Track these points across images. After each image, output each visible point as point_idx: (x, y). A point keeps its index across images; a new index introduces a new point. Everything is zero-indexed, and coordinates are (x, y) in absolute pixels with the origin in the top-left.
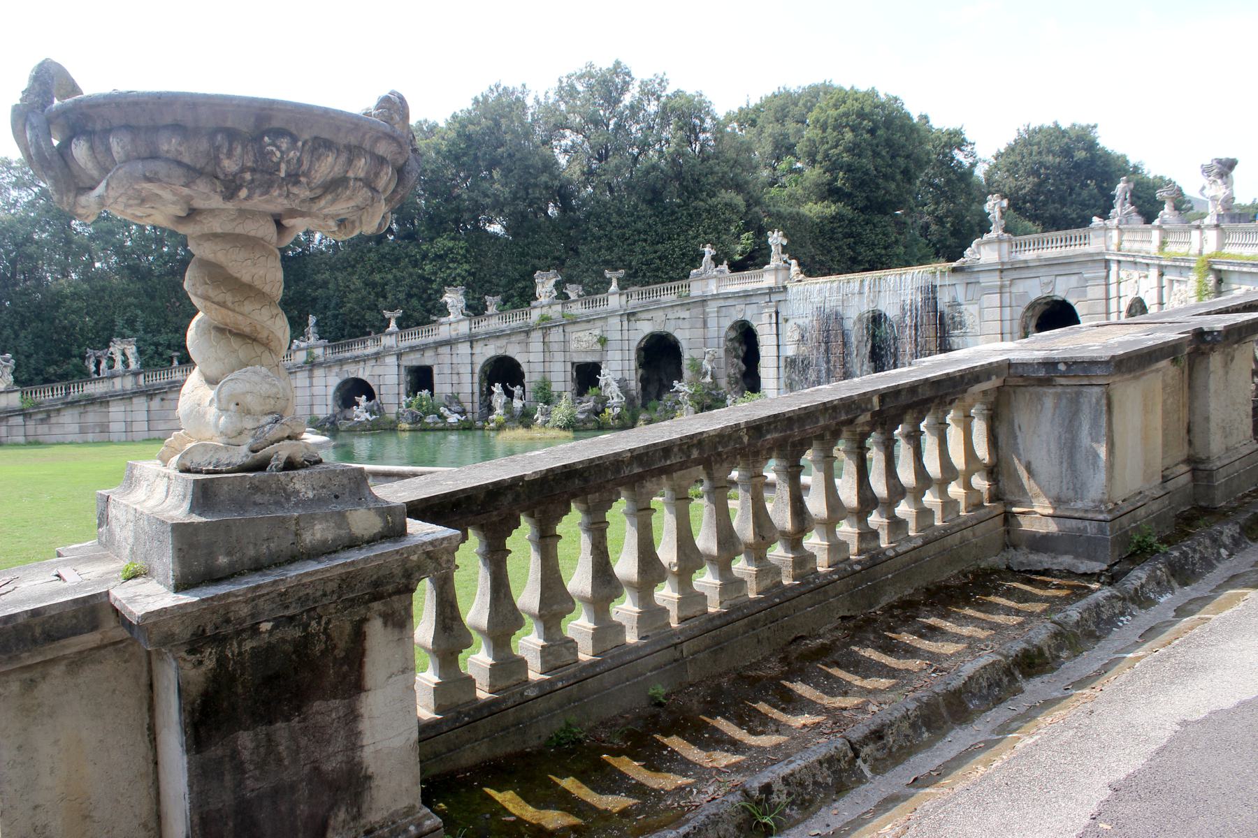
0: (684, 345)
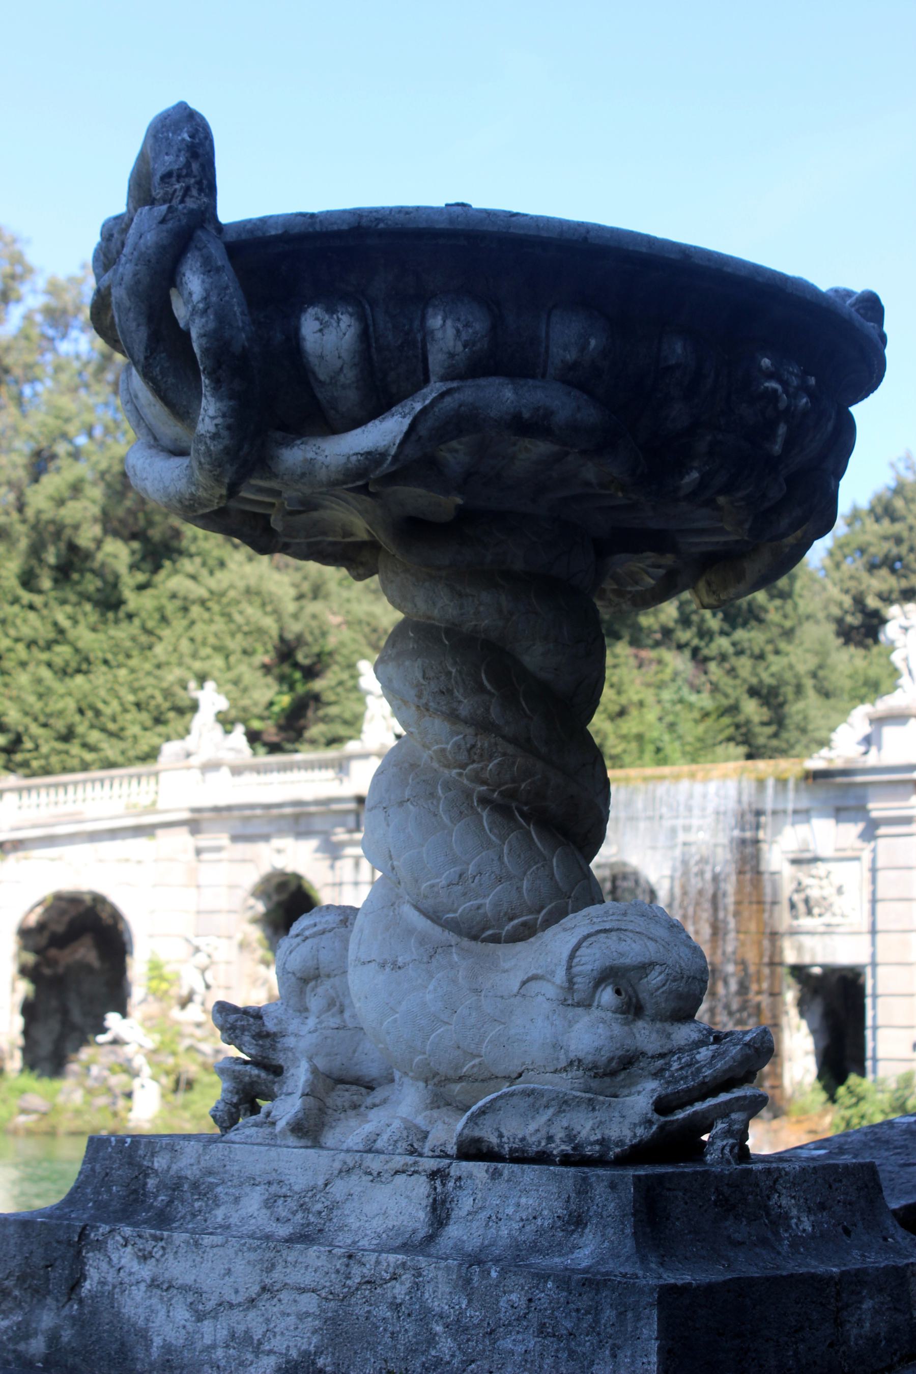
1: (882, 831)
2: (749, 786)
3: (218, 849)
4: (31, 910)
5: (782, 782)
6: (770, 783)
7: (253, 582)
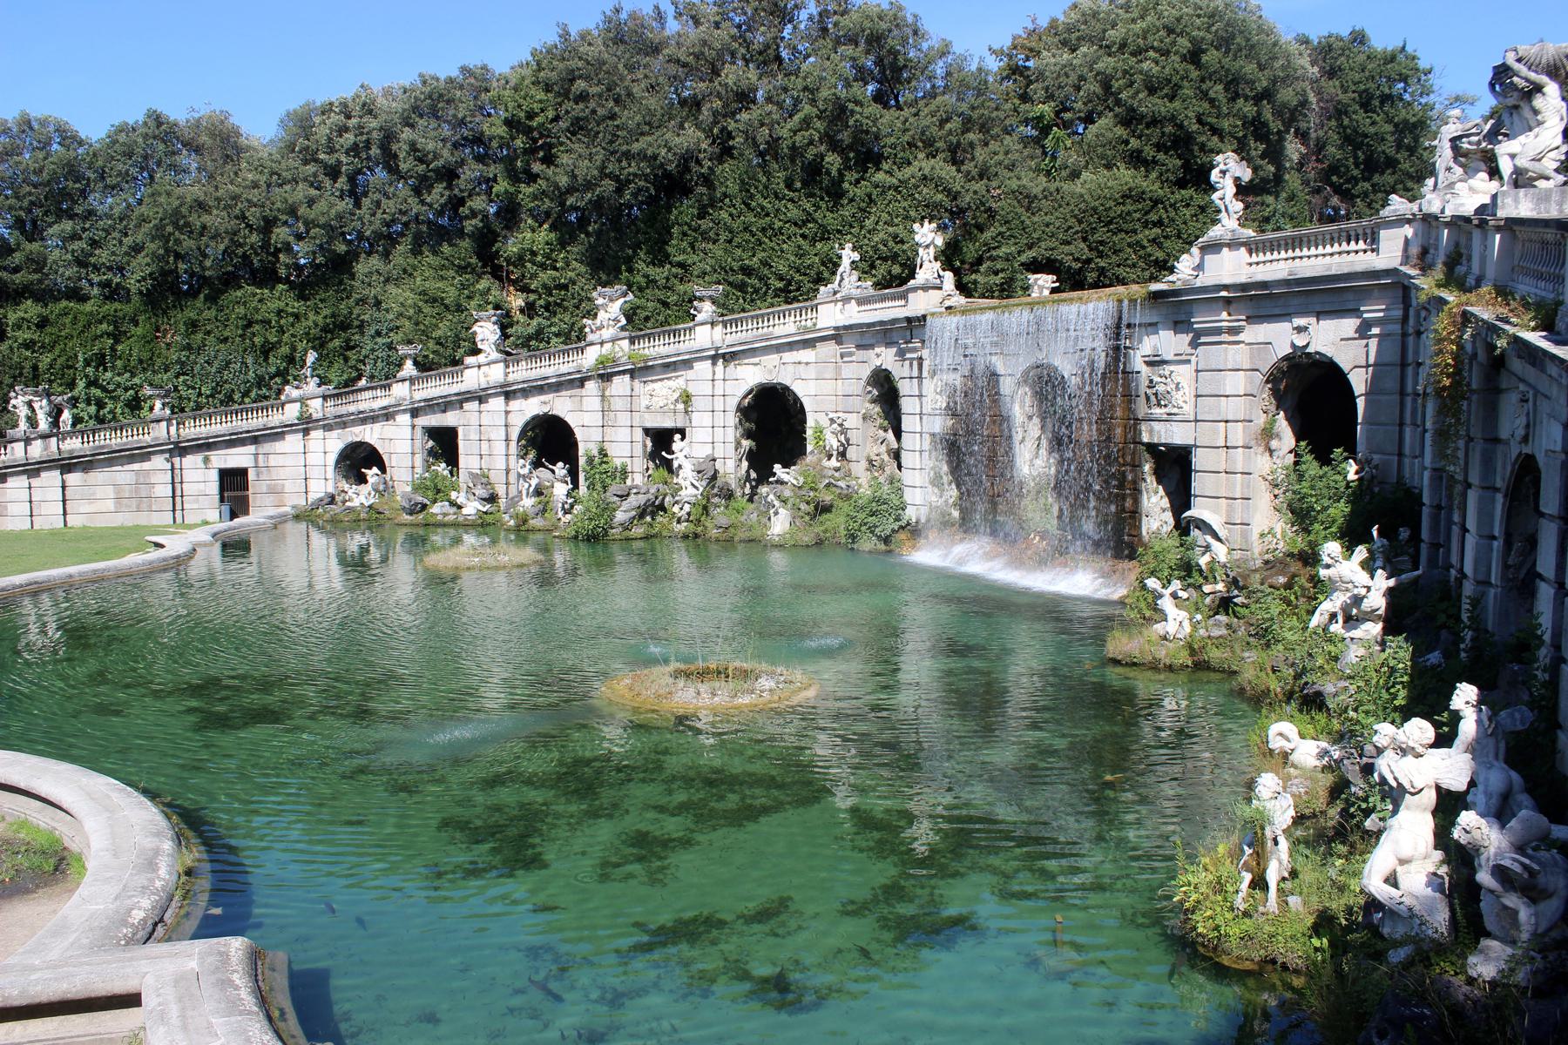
0: (808, 404)
1: (1203, 340)
2: (1112, 305)
3: (851, 354)
4: (745, 397)
5: (1133, 301)
6: (1126, 302)
7: (926, 172)
